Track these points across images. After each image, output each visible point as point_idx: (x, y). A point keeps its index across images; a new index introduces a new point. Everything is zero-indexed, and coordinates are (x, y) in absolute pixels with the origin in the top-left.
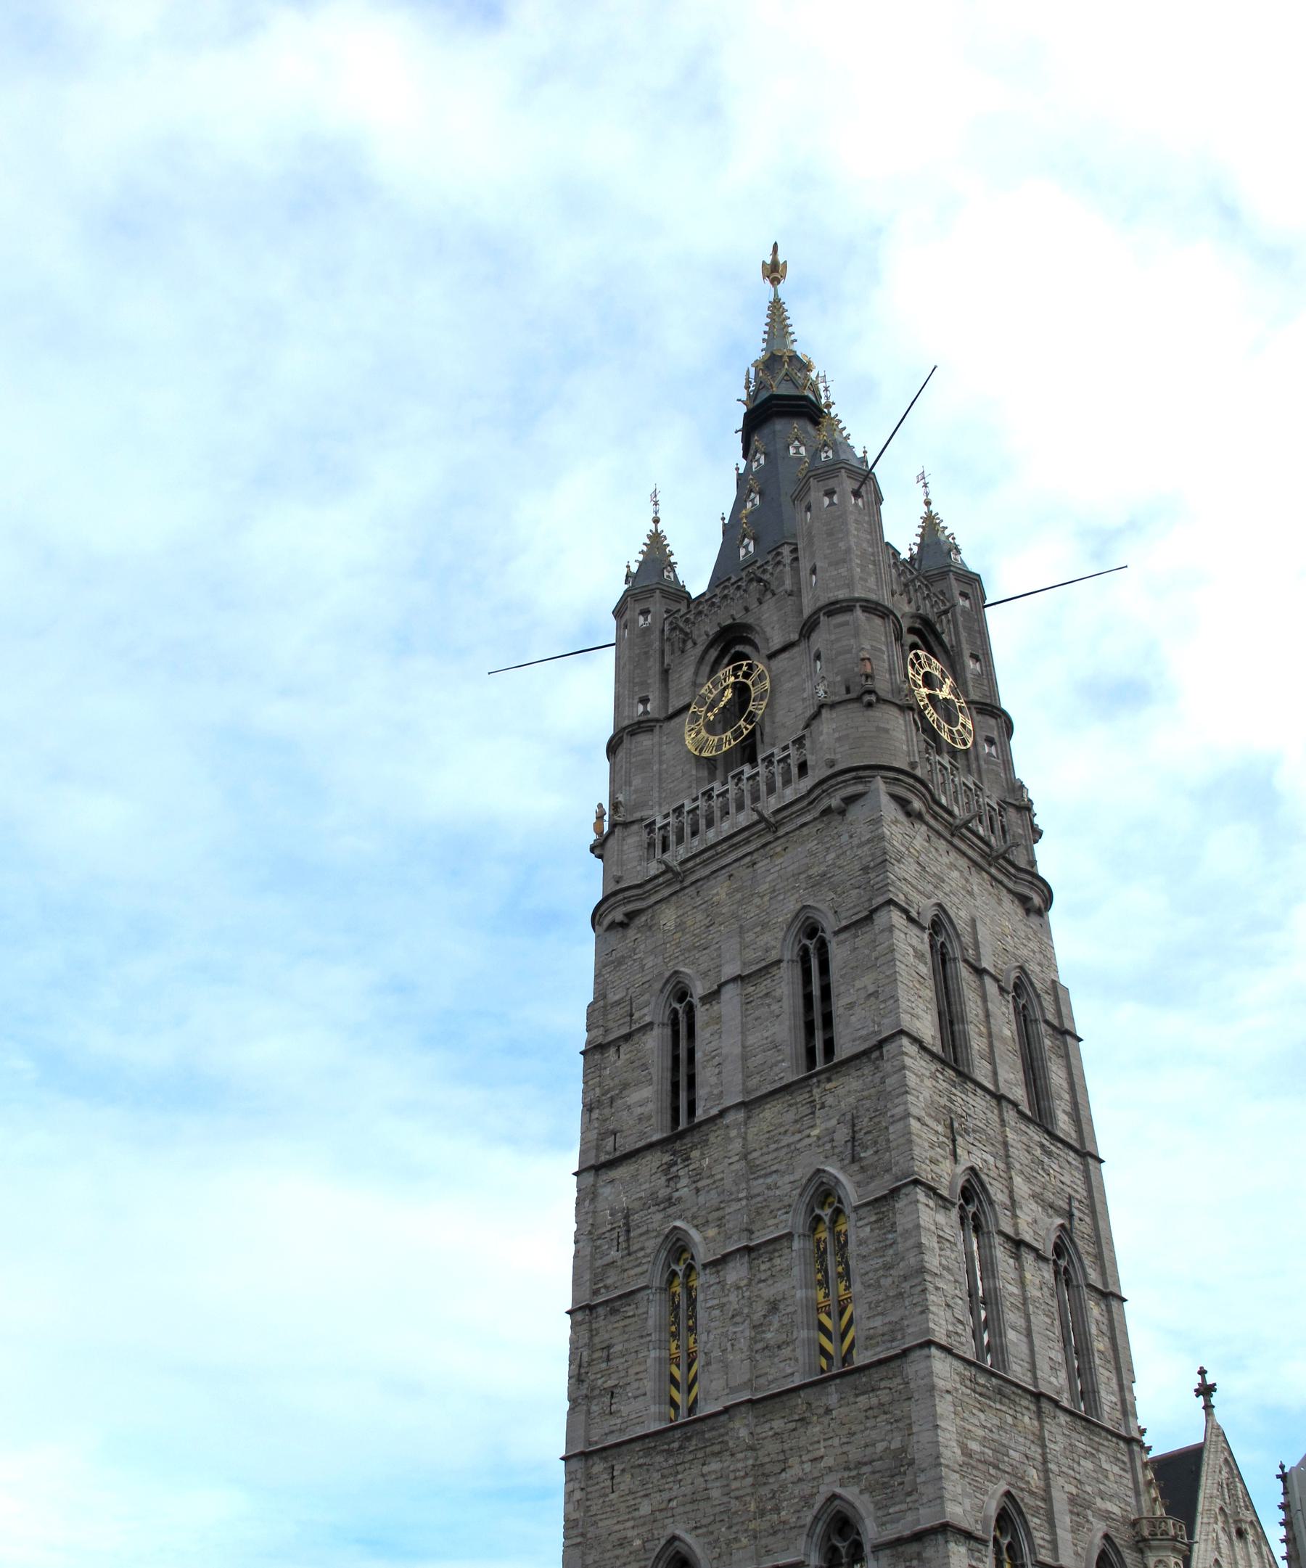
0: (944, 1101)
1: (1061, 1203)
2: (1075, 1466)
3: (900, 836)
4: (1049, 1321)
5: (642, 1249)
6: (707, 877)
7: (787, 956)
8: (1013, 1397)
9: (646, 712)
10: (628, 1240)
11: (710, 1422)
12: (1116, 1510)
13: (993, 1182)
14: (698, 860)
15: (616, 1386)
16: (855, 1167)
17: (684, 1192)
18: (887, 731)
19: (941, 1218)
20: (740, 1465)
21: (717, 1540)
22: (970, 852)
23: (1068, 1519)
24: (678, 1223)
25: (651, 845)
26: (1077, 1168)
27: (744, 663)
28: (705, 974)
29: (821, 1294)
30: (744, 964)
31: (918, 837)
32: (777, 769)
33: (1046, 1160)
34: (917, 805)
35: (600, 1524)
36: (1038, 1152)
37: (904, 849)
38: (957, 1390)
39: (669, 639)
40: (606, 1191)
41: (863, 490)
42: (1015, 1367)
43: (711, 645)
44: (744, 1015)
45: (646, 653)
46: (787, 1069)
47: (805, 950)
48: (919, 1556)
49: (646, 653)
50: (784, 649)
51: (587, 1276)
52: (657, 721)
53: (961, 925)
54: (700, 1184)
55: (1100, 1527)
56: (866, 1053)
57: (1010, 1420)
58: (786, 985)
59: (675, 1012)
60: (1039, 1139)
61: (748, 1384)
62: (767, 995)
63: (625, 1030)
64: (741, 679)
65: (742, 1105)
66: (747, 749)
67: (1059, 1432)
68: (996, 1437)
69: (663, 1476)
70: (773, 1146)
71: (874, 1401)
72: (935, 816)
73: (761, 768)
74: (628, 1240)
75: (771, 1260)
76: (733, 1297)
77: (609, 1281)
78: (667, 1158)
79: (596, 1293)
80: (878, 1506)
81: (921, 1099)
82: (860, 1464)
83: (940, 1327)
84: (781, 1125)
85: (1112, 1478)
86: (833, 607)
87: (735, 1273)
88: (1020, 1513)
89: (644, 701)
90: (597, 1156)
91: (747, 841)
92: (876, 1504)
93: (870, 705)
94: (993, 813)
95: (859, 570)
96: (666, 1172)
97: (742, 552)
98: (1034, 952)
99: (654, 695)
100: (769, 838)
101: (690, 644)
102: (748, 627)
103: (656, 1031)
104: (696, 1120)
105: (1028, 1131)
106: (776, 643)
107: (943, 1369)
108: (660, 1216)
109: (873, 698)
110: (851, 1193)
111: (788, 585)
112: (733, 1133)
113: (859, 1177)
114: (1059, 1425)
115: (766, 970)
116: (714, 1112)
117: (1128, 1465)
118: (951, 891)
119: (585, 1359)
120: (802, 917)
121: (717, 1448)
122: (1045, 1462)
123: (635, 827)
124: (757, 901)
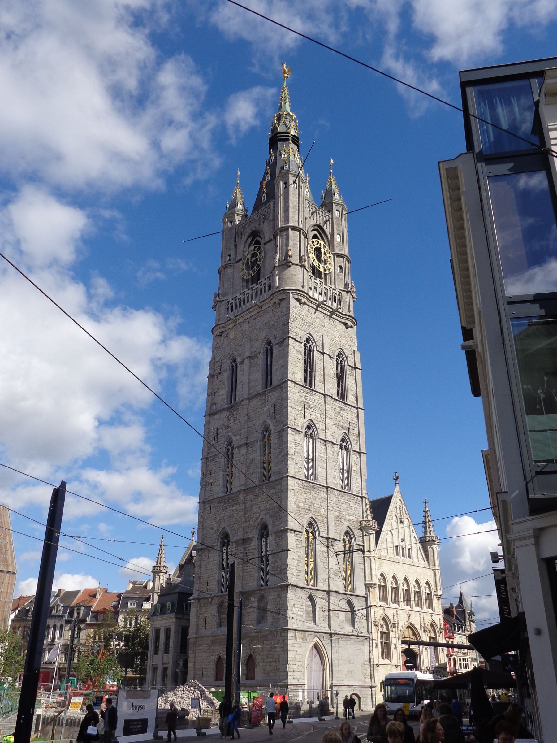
0: (303, 399)
1: (346, 425)
2: (340, 507)
3: (296, 312)
4: (335, 463)
5: (221, 441)
7: (262, 351)
8: (318, 488)
9: (230, 260)
10: (217, 438)
11: (235, 495)
12: (354, 519)
13: (318, 422)
14: (240, 316)
15: (213, 482)
16: (274, 421)
17: (232, 424)
18: (295, 275)
19: (297, 437)
20: (241, 508)
21: (235, 529)
22: (325, 312)
23: (333, 523)
24: (230, 434)
25: (228, 308)
26: (354, 413)
27: (257, 245)
28: (241, 355)
29: (265, 458)
30: (251, 352)
31: (304, 311)
32: (263, 286)
33: (342, 412)
34: (303, 300)
35: (207, 522)
36: (339, 410)
37: (297, 316)
38: (296, 489)
40: (212, 422)
41: (297, 181)
42: (320, 479)
44: (250, 369)
45: (231, 237)
46: (259, 388)
47: (267, 349)
48: (281, 536)
49: (231, 237)
50: (269, 242)
51: (206, 449)
52: (233, 263)
53: (317, 338)
54: (236, 422)
55: (346, 524)
56: (279, 385)
57: (316, 495)
58: (260, 361)
60: (339, 405)
61: (245, 484)
62: (256, 363)
63: (219, 371)
64: (256, 251)
65: (248, 398)
67: (334, 498)
68: (310, 501)
69: (223, 510)
70: (255, 412)
71: (274, 492)
72: (311, 302)
73: (259, 285)
74: (217, 438)
75: (252, 447)
76: (242, 458)
77: (212, 450)
78: (228, 413)
79: (208, 453)
80: (274, 522)
81: (293, 400)
82: (270, 509)
83: (292, 470)
84: (257, 406)
85: (353, 509)
86: (282, 229)
87: (243, 451)
88: (316, 522)
89: (230, 256)
90: (210, 411)
91: (253, 311)
92: (273, 521)
93: (290, 266)
94: (336, 296)
95: (292, 213)
97: (263, 199)
98: (348, 342)
99: (232, 254)
101: (243, 236)
105: (335, 404)
106: (267, 239)
107: (291, 483)
108: (225, 431)
109: (291, 264)
110: (272, 428)
111: (271, 218)
112: (245, 407)
113: (275, 424)
114: (336, 495)
116: (240, 400)
117: (361, 504)
118: (315, 327)
119: (205, 474)
120: (267, 338)
121: (236, 502)
122: (327, 507)
123: (224, 302)
124: (255, 331)
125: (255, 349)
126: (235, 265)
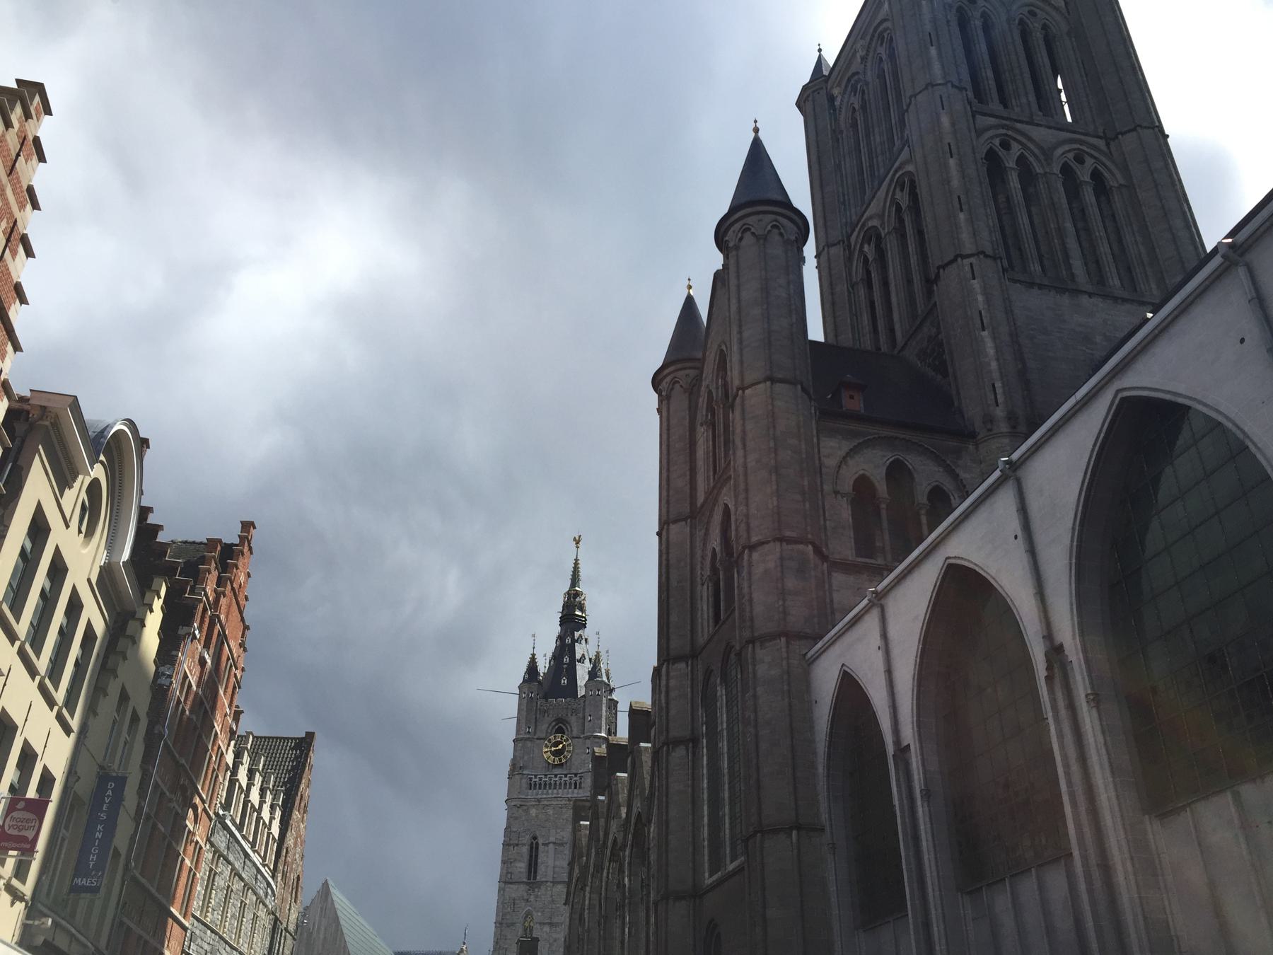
6: (547, 805)
9: (529, 732)
17: (532, 900)
24: (530, 908)
39: (540, 709)
40: (507, 890)
43: (554, 721)
44: (555, 855)
51: (501, 914)
59: (532, 842)
63: (516, 842)
66: (561, 765)
78: (528, 887)
79: (503, 919)
87: (547, 929)
89: (529, 728)
91: (561, 801)
96: (527, 892)
100: (568, 803)
101: (546, 715)
102: (569, 724)
103: (526, 847)
104: (537, 880)
106: (575, 733)
108: (524, 904)
115: (562, 844)
116: (544, 879)
123: (525, 776)
125: (561, 838)
126: (535, 740)
